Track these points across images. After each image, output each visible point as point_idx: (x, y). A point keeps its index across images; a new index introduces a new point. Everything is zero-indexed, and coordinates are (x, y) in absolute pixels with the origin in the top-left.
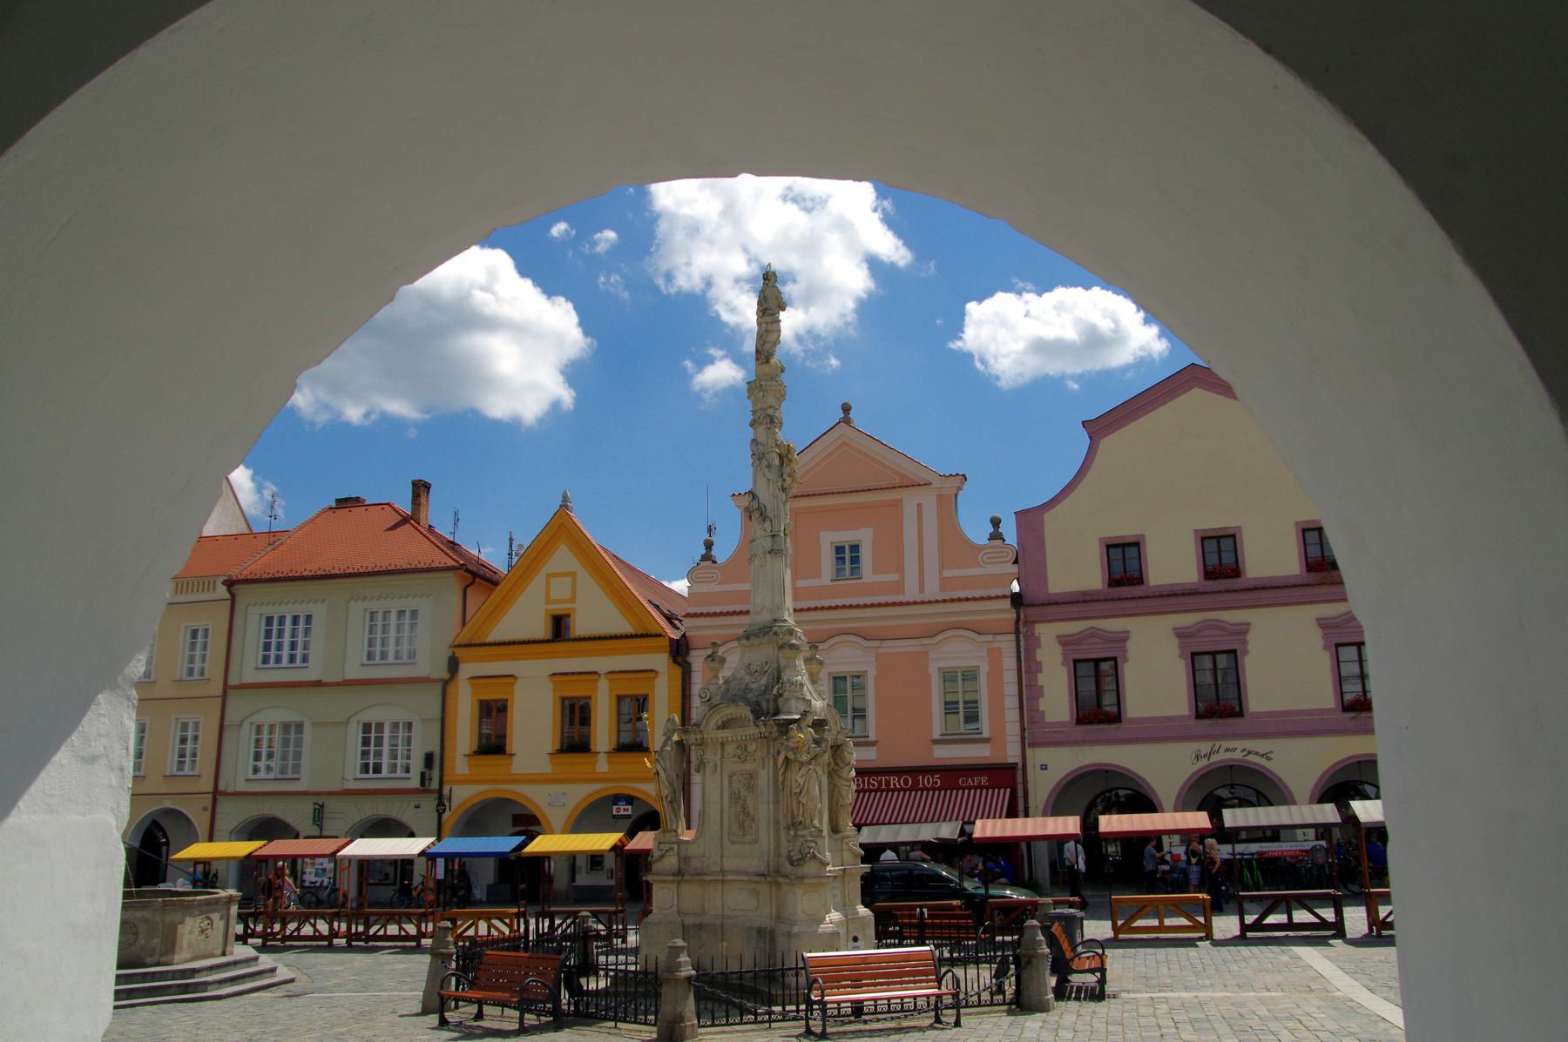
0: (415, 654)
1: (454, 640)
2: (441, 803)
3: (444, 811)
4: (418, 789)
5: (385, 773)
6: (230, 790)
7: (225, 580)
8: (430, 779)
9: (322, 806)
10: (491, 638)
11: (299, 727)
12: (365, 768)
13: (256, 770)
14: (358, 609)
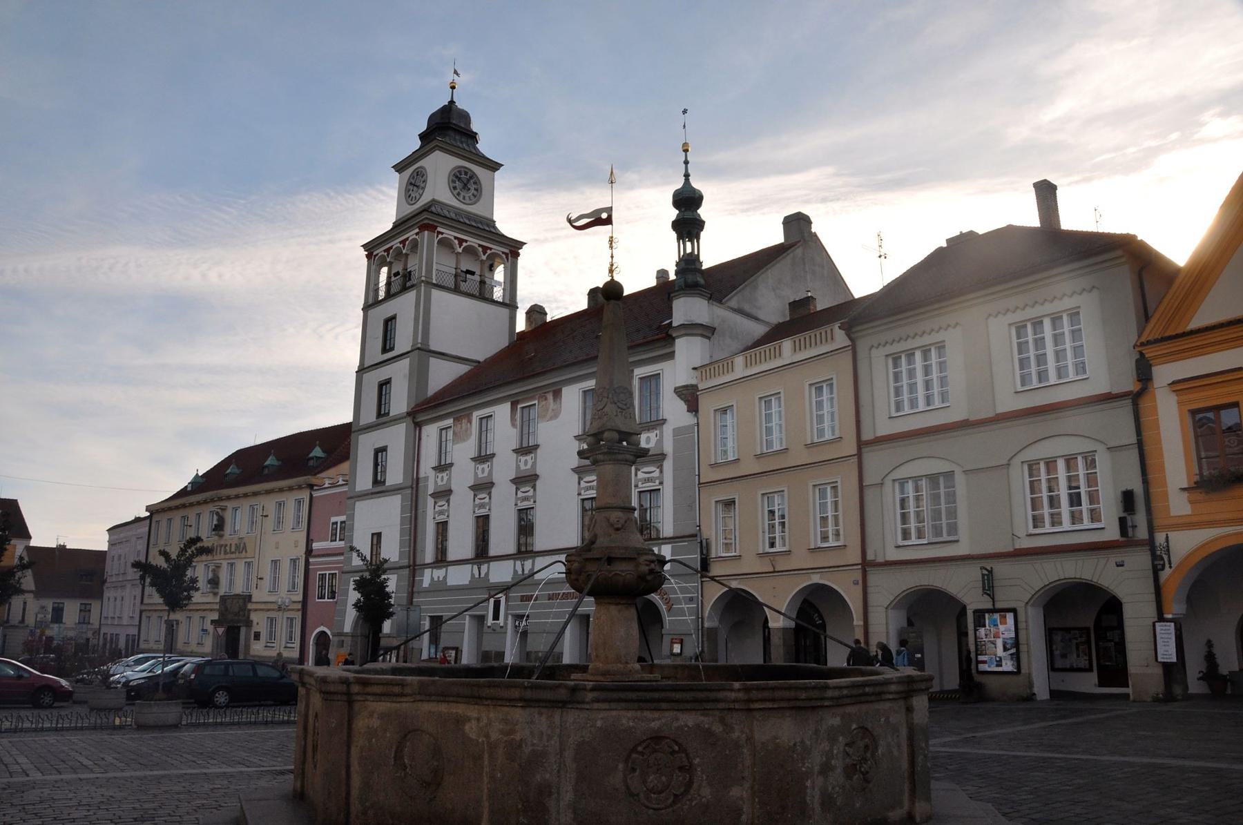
0: (1084, 368)
1: (1139, 337)
2: (1155, 557)
3: (1163, 568)
4: (1118, 541)
5: (1066, 525)
6: (880, 559)
7: (841, 323)
8: (1134, 527)
9: (991, 572)
10: (1194, 324)
11: (949, 475)
12: (1037, 521)
13: (906, 534)
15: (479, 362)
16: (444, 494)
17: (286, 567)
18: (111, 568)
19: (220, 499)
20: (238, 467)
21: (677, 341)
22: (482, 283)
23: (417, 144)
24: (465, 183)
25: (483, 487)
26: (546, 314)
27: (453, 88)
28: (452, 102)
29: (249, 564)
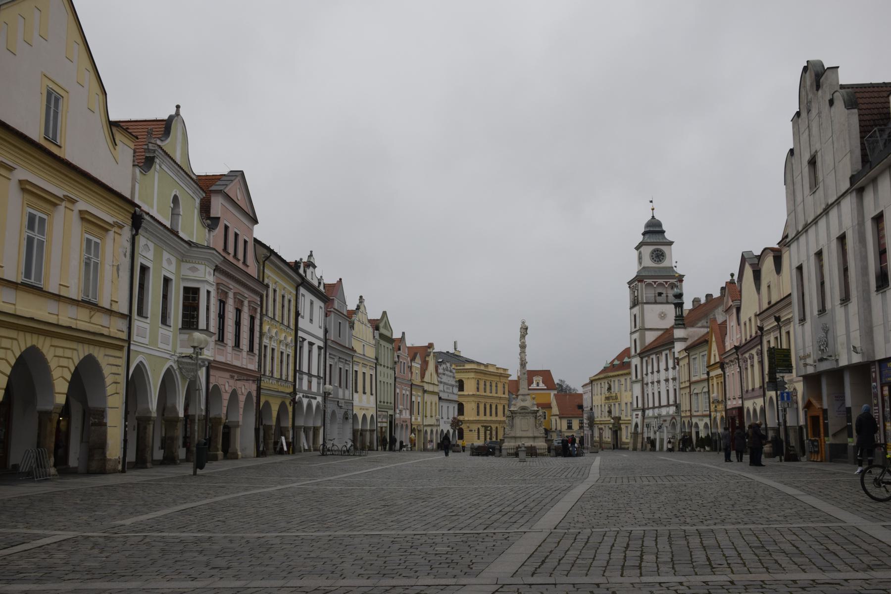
14: (702, 354)
15: (667, 329)
16: (647, 384)
17: (629, 404)
18: (585, 405)
19: (609, 377)
20: (618, 361)
21: (675, 343)
22: (667, 296)
23: (640, 238)
24: (659, 256)
25: (652, 383)
26: (700, 301)
27: (653, 209)
28: (653, 217)
29: (619, 404)
